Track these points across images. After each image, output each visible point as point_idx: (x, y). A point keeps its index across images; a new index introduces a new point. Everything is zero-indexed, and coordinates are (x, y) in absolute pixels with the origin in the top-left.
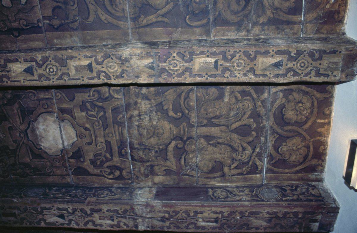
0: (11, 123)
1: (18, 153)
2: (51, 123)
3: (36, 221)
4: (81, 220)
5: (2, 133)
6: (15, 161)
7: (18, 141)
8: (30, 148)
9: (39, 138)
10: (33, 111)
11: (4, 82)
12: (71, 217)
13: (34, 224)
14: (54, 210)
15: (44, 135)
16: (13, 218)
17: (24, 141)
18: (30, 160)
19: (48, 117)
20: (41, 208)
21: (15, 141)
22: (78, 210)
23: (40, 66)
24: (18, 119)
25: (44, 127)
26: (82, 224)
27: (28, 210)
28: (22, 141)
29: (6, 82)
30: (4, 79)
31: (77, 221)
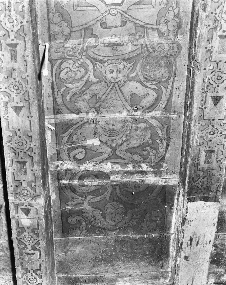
1: (141, 24)
5: (110, 37)
6: (154, 29)
7: (123, 20)
8: (134, 4)
11: (23, 10)
17: (123, 11)
18: (153, 8)
28: (123, 13)
29: (23, 8)
30: (20, 9)
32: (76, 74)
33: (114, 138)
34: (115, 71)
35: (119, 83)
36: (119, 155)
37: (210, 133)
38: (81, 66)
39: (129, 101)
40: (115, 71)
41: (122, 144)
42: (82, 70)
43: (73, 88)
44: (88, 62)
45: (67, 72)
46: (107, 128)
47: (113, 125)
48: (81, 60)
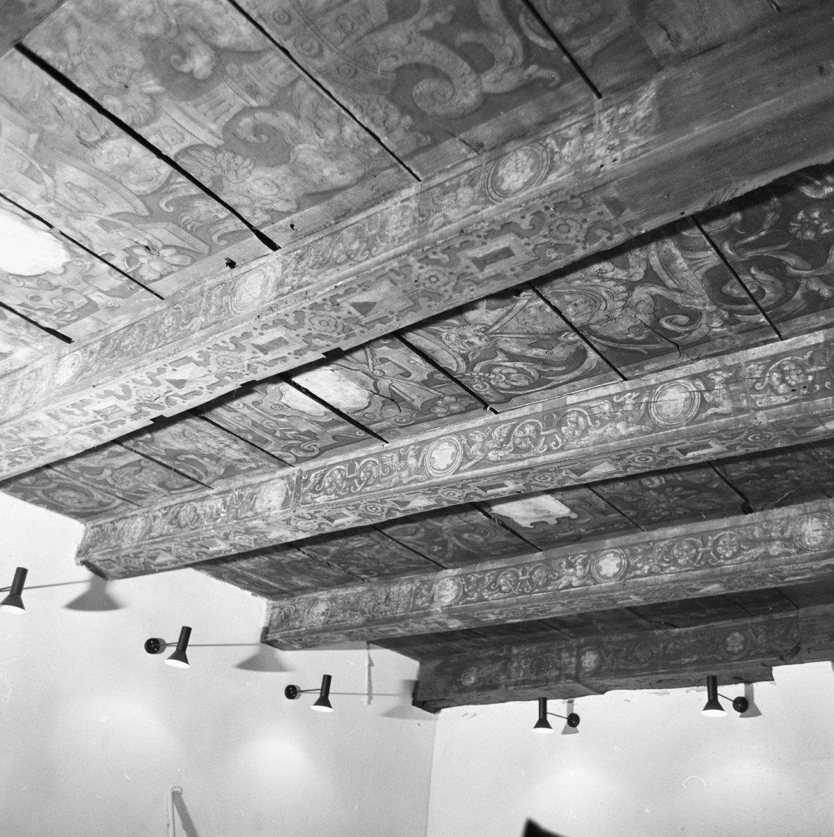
0: (411, 381)
2: (342, 401)
3: (213, 357)
4: (143, 392)
9: (343, 378)
10: (383, 406)
12: (162, 389)
13: (209, 348)
14: (201, 388)
15: (341, 384)
16: (261, 341)
19: (354, 406)
20: (228, 383)
21: (383, 360)
22: (164, 404)
23: (390, 510)
24: (402, 389)
25: (349, 393)
26: (131, 385)
27: (246, 369)
31: (145, 387)
32: (509, 374)
33: (604, 294)
34: (466, 341)
35: (482, 330)
36: (643, 273)
37: (435, 282)
38: (490, 372)
39: (509, 308)
40: (466, 341)
41: (611, 279)
42: (496, 370)
43: (537, 370)
44: (477, 368)
45: (514, 381)
46: (589, 310)
47: (576, 305)
48: (482, 374)
